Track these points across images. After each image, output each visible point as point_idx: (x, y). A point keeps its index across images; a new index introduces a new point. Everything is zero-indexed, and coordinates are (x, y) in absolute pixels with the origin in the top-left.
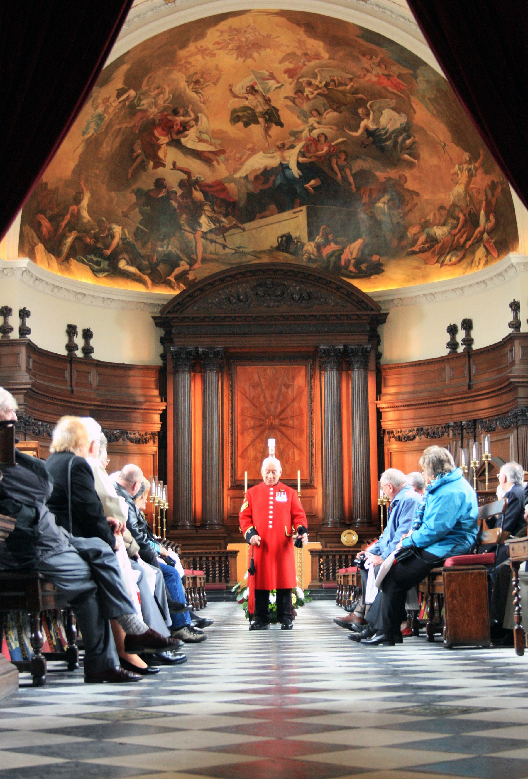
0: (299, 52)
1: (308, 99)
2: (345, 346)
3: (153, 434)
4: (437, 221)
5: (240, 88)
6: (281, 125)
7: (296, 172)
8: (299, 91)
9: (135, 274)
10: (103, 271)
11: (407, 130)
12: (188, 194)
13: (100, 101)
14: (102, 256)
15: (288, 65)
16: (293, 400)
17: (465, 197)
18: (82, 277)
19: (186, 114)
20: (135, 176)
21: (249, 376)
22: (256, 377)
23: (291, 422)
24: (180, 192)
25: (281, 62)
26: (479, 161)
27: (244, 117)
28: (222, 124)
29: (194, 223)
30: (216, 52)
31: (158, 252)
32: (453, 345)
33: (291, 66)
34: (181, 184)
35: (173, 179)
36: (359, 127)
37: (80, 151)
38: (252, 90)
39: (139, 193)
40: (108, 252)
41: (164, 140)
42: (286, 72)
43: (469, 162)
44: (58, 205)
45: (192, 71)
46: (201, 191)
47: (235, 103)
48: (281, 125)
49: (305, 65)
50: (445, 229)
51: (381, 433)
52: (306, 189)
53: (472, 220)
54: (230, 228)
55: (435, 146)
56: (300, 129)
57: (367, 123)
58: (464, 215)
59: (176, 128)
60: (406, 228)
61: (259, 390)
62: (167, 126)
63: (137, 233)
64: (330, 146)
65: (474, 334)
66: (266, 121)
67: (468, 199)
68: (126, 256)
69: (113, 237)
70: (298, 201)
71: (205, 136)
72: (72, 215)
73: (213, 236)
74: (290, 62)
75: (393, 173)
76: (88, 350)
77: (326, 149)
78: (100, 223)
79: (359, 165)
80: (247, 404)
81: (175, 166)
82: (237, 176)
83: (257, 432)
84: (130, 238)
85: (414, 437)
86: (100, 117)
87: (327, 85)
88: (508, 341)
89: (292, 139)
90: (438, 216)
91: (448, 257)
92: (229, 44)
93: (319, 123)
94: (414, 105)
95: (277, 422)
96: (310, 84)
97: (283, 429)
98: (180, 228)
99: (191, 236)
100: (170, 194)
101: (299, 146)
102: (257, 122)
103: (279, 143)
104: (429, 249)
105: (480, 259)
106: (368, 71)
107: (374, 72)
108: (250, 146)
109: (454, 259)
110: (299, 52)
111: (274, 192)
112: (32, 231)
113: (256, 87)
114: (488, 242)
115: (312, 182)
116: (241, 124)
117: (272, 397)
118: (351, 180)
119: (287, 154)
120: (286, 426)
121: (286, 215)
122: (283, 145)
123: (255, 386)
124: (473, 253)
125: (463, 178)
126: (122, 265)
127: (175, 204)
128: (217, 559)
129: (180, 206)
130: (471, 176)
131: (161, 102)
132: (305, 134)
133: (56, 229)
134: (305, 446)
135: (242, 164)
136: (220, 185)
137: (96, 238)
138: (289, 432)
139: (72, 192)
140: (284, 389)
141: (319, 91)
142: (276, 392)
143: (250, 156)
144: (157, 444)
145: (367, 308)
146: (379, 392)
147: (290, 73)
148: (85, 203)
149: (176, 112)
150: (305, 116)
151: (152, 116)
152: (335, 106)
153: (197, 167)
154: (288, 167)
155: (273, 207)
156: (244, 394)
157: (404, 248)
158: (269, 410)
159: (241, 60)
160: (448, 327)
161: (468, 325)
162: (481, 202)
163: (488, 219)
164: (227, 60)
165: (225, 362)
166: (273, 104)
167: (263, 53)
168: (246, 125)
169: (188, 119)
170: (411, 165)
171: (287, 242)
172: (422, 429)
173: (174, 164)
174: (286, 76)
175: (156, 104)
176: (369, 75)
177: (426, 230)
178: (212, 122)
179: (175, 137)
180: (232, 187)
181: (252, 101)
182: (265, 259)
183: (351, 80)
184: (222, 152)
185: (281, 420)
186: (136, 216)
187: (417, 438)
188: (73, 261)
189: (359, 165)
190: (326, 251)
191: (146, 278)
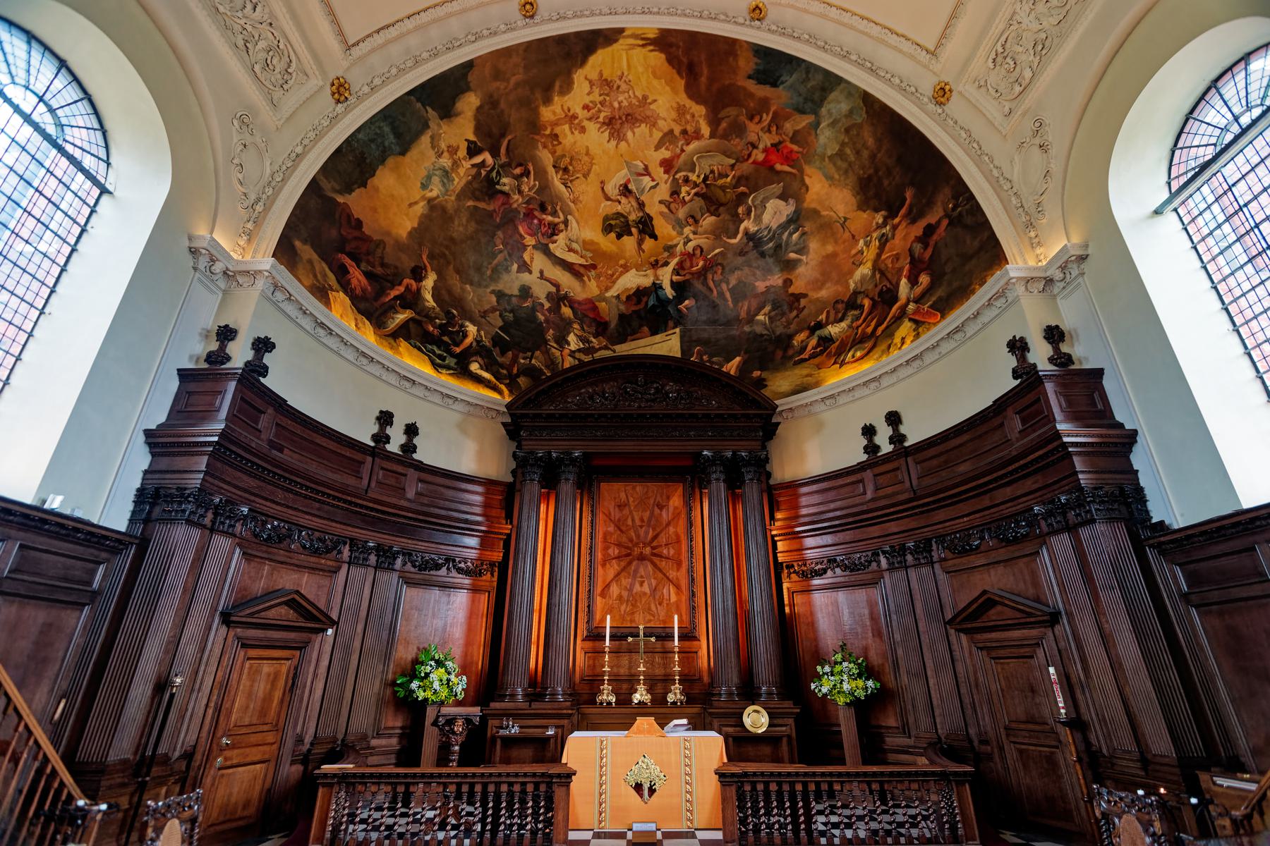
0: (677, 131)
1: (684, 202)
2: (734, 453)
3: (492, 564)
4: (831, 319)
5: (612, 189)
7: (669, 292)
8: (675, 193)
9: (489, 381)
10: (448, 368)
11: (795, 220)
12: (556, 309)
15: (665, 154)
16: (668, 524)
17: (874, 275)
18: (414, 362)
20: (496, 274)
21: (613, 493)
22: (623, 495)
23: (665, 551)
24: (547, 305)
25: (657, 148)
26: (903, 211)
27: (616, 226)
29: (562, 341)
30: (586, 123)
31: (519, 363)
32: (872, 449)
34: (549, 296)
35: (541, 291)
36: (737, 232)
38: (626, 191)
39: (500, 295)
40: (458, 350)
41: (530, 241)
43: (885, 224)
44: (383, 265)
45: (559, 151)
46: (571, 307)
47: (607, 208)
49: (683, 151)
50: (844, 325)
52: (679, 311)
53: (888, 296)
54: (600, 349)
56: (675, 242)
57: (748, 225)
58: (872, 299)
60: (791, 337)
61: (626, 511)
63: (496, 340)
64: (705, 260)
65: (903, 429)
66: (640, 232)
67: (878, 276)
69: (465, 335)
70: (671, 323)
71: (575, 246)
72: (407, 288)
74: (667, 149)
76: (409, 448)
77: (701, 263)
78: (448, 313)
80: (611, 528)
81: (542, 276)
82: (608, 294)
83: (623, 564)
85: (825, 571)
86: (446, 174)
87: (706, 178)
89: (666, 254)
91: (850, 355)
92: (600, 111)
93: (695, 233)
94: (807, 180)
95: (648, 550)
96: (686, 180)
97: (656, 560)
98: (546, 342)
99: (558, 353)
100: (537, 306)
101: (674, 263)
102: (630, 234)
103: (652, 259)
104: (822, 352)
105: (903, 339)
106: (754, 146)
107: (761, 146)
108: (622, 262)
110: (677, 131)
112: (324, 265)
113: (630, 186)
114: (916, 312)
115: (687, 302)
116: (613, 235)
117: (642, 520)
118: (728, 295)
119: (660, 272)
120: (660, 556)
121: (658, 338)
122: (657, 261)
123: (621, 506)
124: (892, 335)
125: (870, 254)
127: (542, 318)
128: (530, 788)
129: (547, 321)
130: (884, 241)
131: (525, 189)
132: (680, 248)
133: (381, 292)
134: (684, 583)
135: (614, 282)
136: (591, 304)
137: (442, 328)
138: (663, 564)
139: (407, 263)
140: (657, 511)
142: (646, 515)
143: (622, 274)
144: (495, 578)
147: (667, 165)
148: (429, 282)
149: (543, 208)
150: (679, 225)
151: (515, 206)
152: (712, 209)
154: (661, 287)
155: (646, 329)
156: (608, 516)
157: (791, 357)
158: (638, 536)
159: (613, 143)
160: (863, 429)
161: (894, 419)
164: (594, 138)
166: (647, 210)
168: (619, 236)
169: (557, 220)
172: (835, 561)
173: (541, 272)
174: (662, 170)
175: (520, 192)
176: (755, 151)
177: (818, 333)
178: (582, 230)
179: (544, 241)
181: (626, 206)
183: (733, 166)
184: (594, 267)
185: (653, 548)
187: (829, 573)
188: (403, 345)
191: (502, 387)
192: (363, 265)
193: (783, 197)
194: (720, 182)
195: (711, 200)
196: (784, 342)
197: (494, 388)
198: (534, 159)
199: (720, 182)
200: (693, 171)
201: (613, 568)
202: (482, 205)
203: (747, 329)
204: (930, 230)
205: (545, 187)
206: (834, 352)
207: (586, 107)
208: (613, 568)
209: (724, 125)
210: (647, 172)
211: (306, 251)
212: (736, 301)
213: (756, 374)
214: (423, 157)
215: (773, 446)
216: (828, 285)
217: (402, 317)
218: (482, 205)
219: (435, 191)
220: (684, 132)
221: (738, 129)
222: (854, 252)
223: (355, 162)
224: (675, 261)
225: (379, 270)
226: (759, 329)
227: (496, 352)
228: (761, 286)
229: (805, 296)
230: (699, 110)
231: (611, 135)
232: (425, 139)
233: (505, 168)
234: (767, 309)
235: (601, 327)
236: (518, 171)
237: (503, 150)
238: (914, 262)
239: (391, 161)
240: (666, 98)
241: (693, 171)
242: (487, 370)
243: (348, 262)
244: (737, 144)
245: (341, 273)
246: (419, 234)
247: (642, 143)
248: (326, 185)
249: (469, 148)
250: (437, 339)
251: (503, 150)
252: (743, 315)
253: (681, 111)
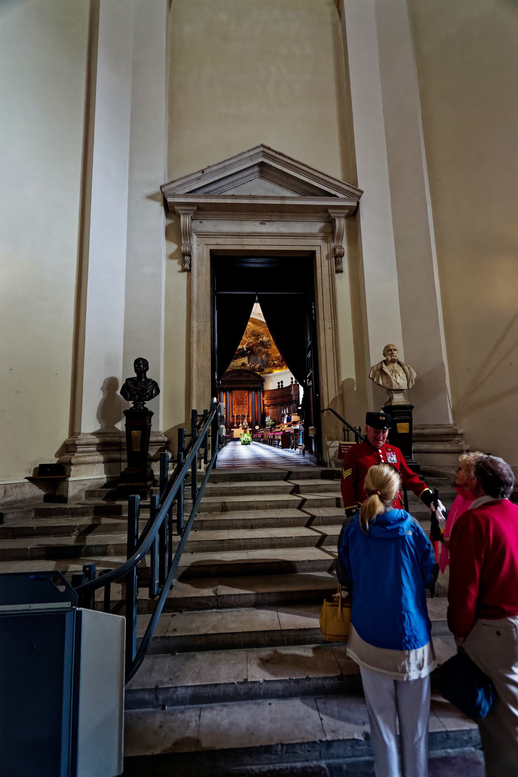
7: (245, 349)
21: (236, 393)
32: (279, 386)
51: (264, 405)
75: (266, 350)
79: (259, 348)
88: (291, 386)
123: (237, 395)
146: (263, 397)
150: (247, 338)
161: (282, 382)
165: (230, 390)
170: (270, 348)
171: (243, 364)
182: (239, 368)
189: (259, 348)
190: (252, 366)
201: (235, 406)
206: (276, 366)
208: (235, 406)
215: (264, 383)
228: (264, 350)
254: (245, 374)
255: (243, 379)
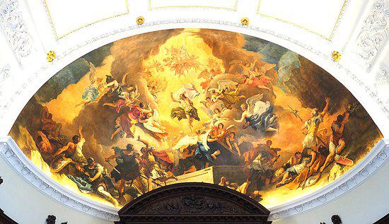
0: (209, 70)
4: (295, 162)
5: (177, 96)
6: (199, 120)
7: (206, 148)
8: (208, 98)
10: (87, 190)
11: (270, 111)
12: (145, 157)
13: (95, 78)
14: (87, 180)
17: (315, 139)
19: (147, 108)
20: (115, 139)
25: (199, 77)
27: (179, 114)
28: (166, 117)
29: (148, 174)
30: (164, 67)
31: (124, 187)
33: (204, 80)
35: (138, 147)
37: (81, 108)
38: (183, 97)
39: (117, 149)
40: (93, 180)
41: (134, 121)
42: (201, 85)
43: (317, 114)
44: (59, 136)
45: (151, 79)
48: (199, 120)
49: (212, 78)
50: (302, 165)
52: (212, 157)
53: (324, 151)
54: (169, 178)
55: (292, 115)
56: (209, 121)
57: (247, 113)
59: (141, 116)
60: (273, 172)
62: (137, 115)
63: (113, 174)
67: (317, 140)
68: (104, 185)
69: (97, 172)
70: (207, 164)
71: (156, 124)
73: (159, 182)
78: (89, 160)
79: (240, 141)
84: (108, 175)
87: (223, 91)
89: (204, 128)
90: (295, 159)
93: (219, 117)
94: (275, 93)
96: (214, 92)
98: (140, 175)
101: (208, 132)
103: (197, 131)
104: (292, 180)
106: (247, 77)
107: (251, 77)
108: (181, 132)
109: (312, 182)
111: (195, 158)
112: (31, 137)
114: (340, 159)
115: (216, 153)
116: (176, 118)
118: (238, 149)
122: (199, 131)
124: (329, 172)
125: (312, 129)
126: (101, 189)
127: (138, 162)
130: (317, 125)
131: (133, 97)
133: (55, 151)
139: (72, 134)
141: (219, 96)
143: (181, 137)
145: (260, 212)
147: (204, 85)
149: (141, 106)
150: (211, 113)
153: (152, 142)
157: (275, 183)
159: (177, 75)
162: (328, 138)
163: (336, 144)
164: (168, 74)
167: (190, 71)
168: (180, 119)
169: (148, 111)
173: (139, 137)
177: (288, 169)
178: (161, 115)
180: (171, 155)
183: (237, 86)
184: (166, 134)
186: (114, 163)
188: (65, 177)
191: (115, 200)
192: (50, 136)
193: (264, 100)
194: (231, 93)
195: (227, 102)
196: (270, 174)
197: (111, 201)
198: (139, 83)
199: (231, 93)
200: (217, 87)
202: (111, 105)
203: (249, 167)
204: (340, 119)
205: (142, 96)
207: (165, 60)
209: (232, 68)
210: (194, 88)
211: (24, 131)
212: (242, 153)
213: (256, 192)
214: (85, 82)
216: (292, 144)
217: (65, 162)
218: (111, 105)
219: (89, 98)
220: (213, 70)
221: (239, 70)
222: (302, 127)
223: (52, 89)
224: (210, 130)
225: (57, 138)
226: (256, 168)
227: (113, 180)
228: (255, 144)
229: (280, 150)
230: (220, 61)
231: (177, 72)
232: (87, 76)
233: (124, 87)
234: (260, 156)
235: (170, 166)
236: (130, 88)
237: (124, 79)
238: (334, 133)
239: (69, 87)
240: (204, 56)
241: (217, 87)
242: (107, 191)
243: (43, 135)
244: (239, 77)
245: (38, 140)
246: (77, 120)
247: (193, 77)
248: (38, 99)
249: (107, 79)
250: (82, 173)
251: (124, 79)
252: (247, 159)
253: (211, 62)
254: (208, 200)
255: (203, 213)
